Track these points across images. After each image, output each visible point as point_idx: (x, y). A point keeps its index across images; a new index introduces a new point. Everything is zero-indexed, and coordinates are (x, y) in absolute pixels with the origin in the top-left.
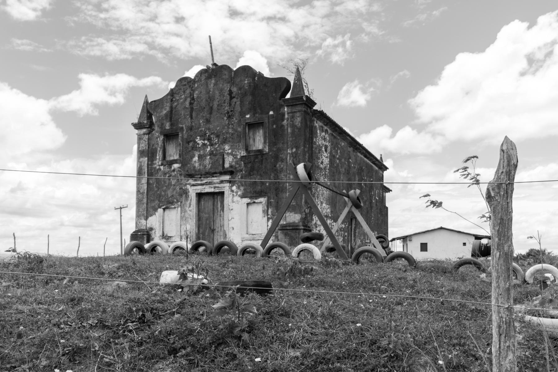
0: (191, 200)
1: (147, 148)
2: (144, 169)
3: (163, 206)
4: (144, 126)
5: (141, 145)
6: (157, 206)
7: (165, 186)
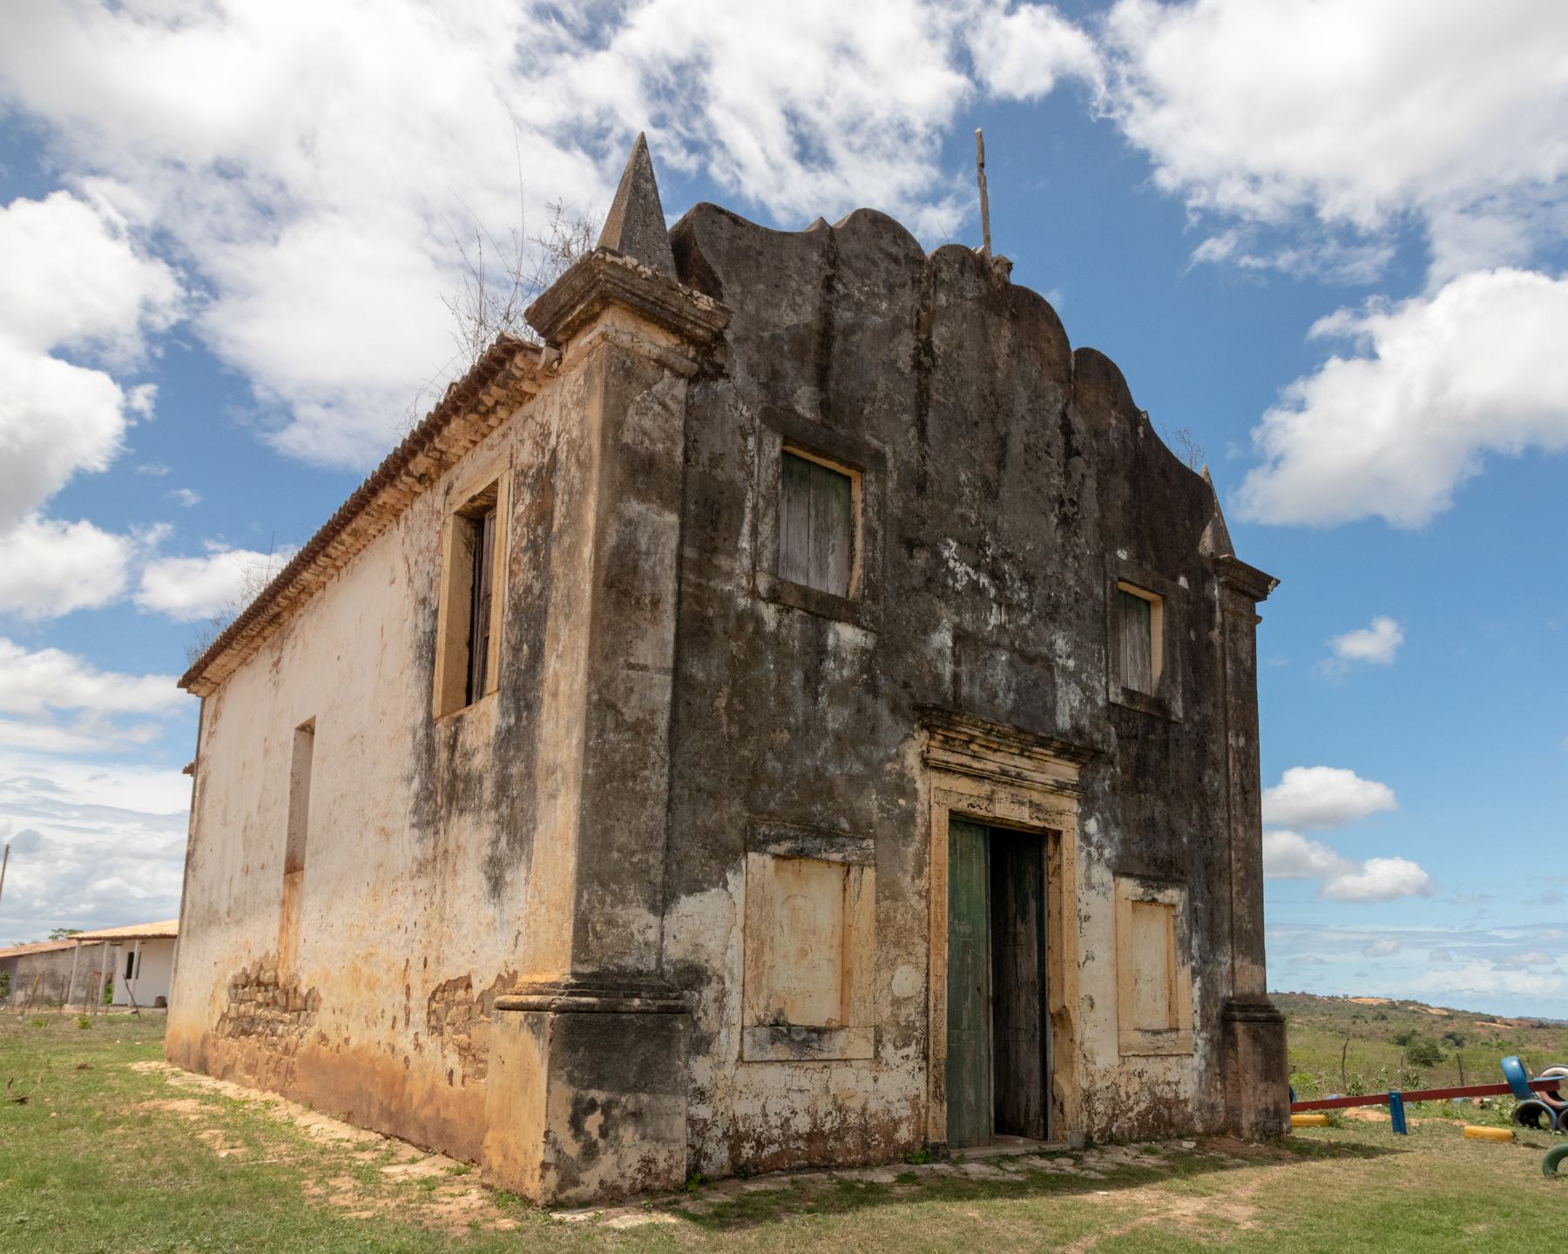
0: (928, 834)
3: (778, 840)
6: (734, 837)
7: (789, 730)
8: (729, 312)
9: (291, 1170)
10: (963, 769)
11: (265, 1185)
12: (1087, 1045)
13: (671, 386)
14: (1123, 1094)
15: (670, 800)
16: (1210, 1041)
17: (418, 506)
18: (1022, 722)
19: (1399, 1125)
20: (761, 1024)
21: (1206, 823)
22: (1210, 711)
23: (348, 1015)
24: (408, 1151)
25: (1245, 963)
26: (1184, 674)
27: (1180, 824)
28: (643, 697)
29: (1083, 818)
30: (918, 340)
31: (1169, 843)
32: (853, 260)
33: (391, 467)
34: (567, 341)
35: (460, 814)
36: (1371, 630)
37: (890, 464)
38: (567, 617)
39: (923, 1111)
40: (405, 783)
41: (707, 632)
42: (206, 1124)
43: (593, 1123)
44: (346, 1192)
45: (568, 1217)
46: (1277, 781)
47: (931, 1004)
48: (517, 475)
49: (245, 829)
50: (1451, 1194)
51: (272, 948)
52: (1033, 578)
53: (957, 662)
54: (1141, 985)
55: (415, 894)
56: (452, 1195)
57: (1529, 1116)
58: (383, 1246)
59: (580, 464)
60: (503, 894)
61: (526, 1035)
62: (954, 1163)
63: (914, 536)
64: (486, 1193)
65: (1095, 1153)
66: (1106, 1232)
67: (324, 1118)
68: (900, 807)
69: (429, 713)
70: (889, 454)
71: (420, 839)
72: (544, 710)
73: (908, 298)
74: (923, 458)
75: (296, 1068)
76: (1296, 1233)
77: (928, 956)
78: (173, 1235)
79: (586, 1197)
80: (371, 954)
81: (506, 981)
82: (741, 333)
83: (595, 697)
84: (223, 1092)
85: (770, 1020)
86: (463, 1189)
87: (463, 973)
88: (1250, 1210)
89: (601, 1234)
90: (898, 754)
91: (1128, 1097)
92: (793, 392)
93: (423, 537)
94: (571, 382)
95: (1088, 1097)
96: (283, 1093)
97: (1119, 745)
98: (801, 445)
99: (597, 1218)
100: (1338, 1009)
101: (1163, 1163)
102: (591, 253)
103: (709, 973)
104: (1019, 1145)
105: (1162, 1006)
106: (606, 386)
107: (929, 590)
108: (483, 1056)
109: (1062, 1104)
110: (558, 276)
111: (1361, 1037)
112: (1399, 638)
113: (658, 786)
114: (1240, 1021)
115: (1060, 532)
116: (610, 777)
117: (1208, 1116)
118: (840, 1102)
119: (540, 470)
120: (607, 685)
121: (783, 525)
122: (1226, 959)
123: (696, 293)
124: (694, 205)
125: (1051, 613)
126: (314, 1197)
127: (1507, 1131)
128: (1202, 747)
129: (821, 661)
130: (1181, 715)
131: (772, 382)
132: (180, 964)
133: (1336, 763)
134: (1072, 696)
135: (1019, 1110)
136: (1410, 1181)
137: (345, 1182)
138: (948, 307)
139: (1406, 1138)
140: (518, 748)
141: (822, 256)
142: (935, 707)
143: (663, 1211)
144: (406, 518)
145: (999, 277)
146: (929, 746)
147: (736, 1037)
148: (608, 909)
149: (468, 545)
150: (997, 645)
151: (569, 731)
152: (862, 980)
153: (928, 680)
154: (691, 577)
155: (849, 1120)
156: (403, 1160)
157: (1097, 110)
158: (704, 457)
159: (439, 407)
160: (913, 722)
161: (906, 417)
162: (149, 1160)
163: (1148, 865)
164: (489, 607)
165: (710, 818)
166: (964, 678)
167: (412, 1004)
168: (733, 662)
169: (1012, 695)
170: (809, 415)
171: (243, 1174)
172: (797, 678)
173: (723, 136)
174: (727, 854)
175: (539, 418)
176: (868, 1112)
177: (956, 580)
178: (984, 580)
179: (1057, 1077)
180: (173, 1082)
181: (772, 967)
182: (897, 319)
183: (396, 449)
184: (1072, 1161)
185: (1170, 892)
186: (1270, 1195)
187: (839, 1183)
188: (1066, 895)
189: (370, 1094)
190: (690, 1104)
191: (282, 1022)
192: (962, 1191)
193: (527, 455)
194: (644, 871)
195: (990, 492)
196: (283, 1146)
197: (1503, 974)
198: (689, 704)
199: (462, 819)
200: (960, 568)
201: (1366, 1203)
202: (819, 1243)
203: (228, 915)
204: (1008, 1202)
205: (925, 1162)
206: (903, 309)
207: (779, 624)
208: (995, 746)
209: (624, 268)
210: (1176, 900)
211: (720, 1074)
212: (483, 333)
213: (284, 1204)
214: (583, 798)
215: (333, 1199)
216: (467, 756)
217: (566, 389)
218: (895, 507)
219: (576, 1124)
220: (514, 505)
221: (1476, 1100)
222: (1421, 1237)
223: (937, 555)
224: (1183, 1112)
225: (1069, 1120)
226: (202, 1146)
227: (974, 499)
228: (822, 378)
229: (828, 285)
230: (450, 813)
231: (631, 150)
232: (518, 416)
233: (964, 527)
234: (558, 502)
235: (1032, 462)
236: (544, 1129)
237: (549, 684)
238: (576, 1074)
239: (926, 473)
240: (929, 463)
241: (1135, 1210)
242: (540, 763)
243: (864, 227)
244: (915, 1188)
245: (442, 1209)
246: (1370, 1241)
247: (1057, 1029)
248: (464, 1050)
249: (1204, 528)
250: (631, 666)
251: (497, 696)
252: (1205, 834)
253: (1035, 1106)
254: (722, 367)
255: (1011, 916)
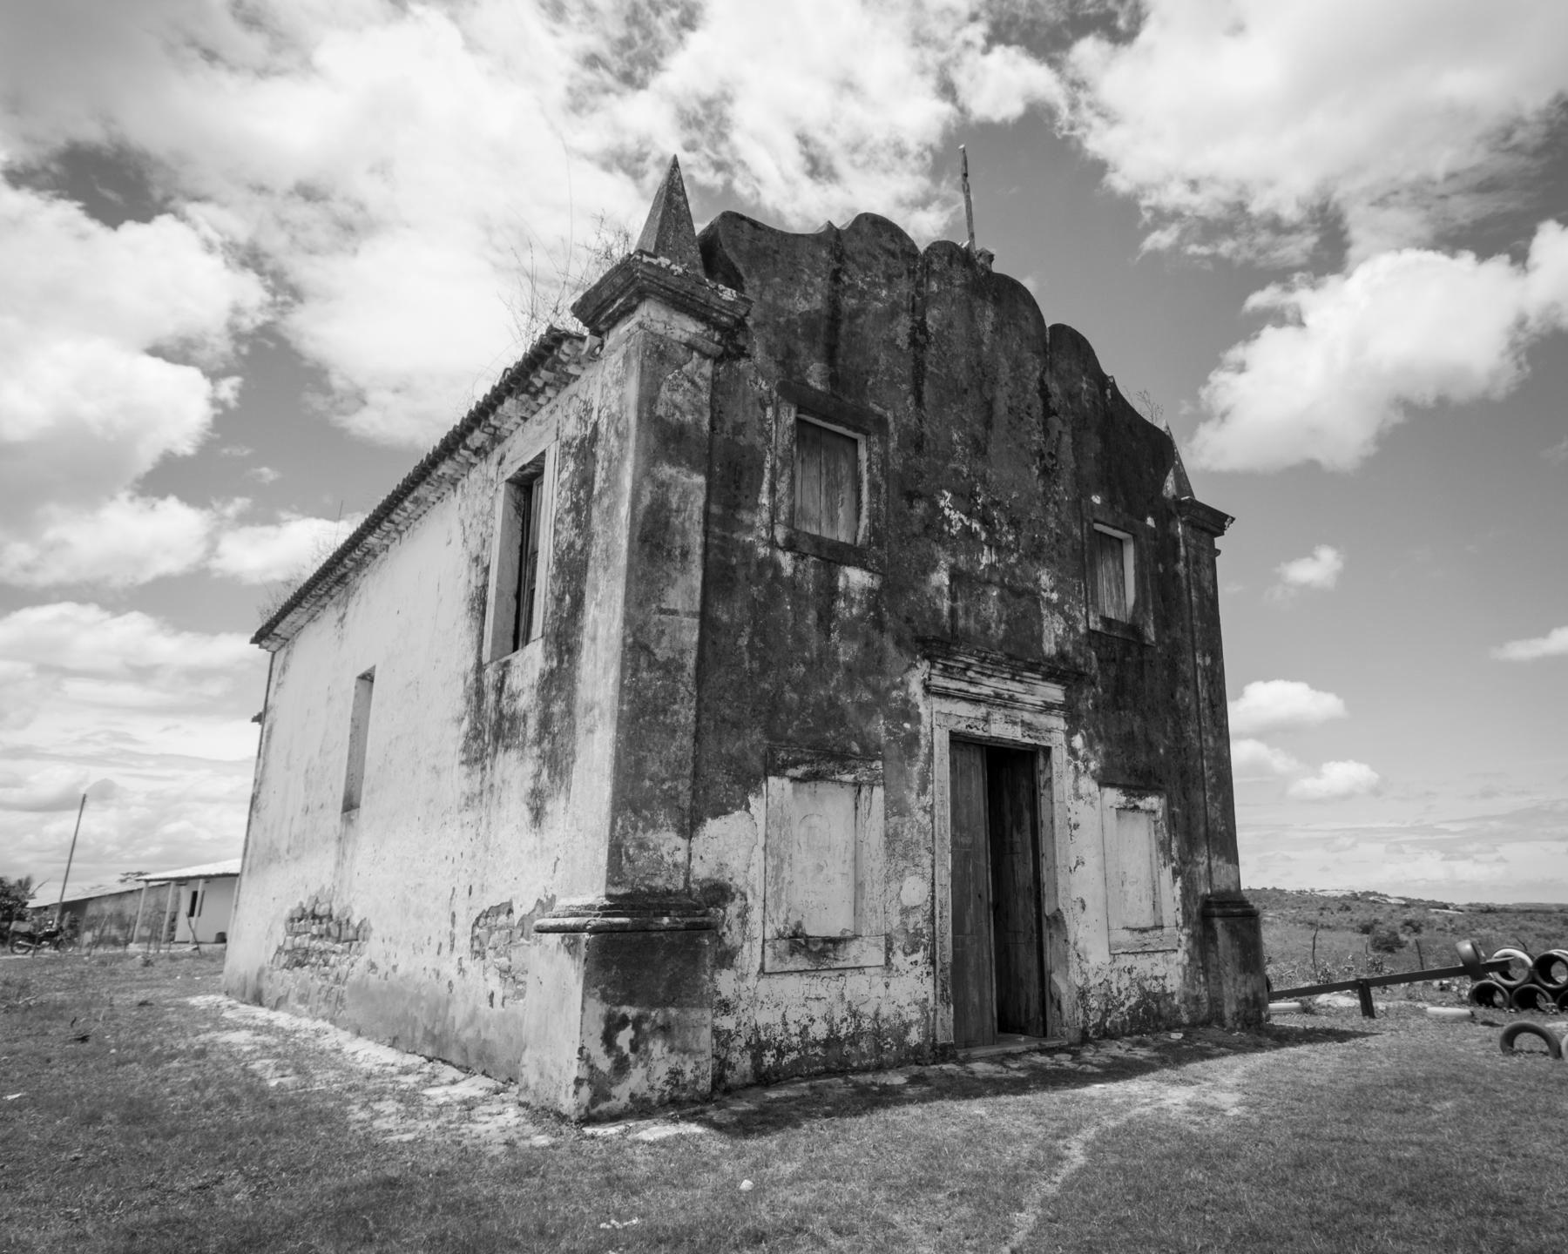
1: (706, 426)
2: (684, 534)
3: (795, 764)
4: (706, 306)
5: (665, 393)
8: (749, 302)
9: (338, 1096)
10: (961, 694)
11: (312, 1112)
12: (1080, 945)
13: (699, 366)
14: (1115, 990)
15: (698, 731)
16: (1191, 937)
17: (474, 475)
18: (1012, 650)
19: (1368, 1009)
20: (780, 936)
21: (1180, 736)
22: (1179, 635)
23: (397, 943)
24: (450, 1073)
25: (1220, 863)
26: (1154, 602)
27: (1156, 736)
28: (673, 638)
29: (1070, 734)
30: (914, 321)
31: (1148, 755)
32: (856, 255)
33: (450, 442)
34: (608, 330)
35: (506, 751)
36: (1315, 558)
37: (892, 427)
38: (606, 569)
39: (931, 1014)
40: (455, 724)
41: (731, 579)
42: (258, 1054)
43: (624, 1038)
44: (390, 1116)
45: (600, 1131)
46: (1240, 694)
47: (937, 912)
48: (562, 446)
49: (307, 771)
50: (1419, 1074)
51: (327, 882)
52: (1019, 522)
53: (954, 598)
54: (1127, 887)
55: (462, 826)
56: (490, 1114)
57: (1483, 996)
58: (423, 1168)
59: (618, 434)
60: (543, 824)
61: (563, 957)
62: (961, 1063)
63: (912, 489)
64: (522, 1111)
65: (1091, 1047)
66: (1104, 1124)
67: (371, 1043)
68: (905, 730)
69: (479, 659)
70: (891, 419)
71: (469, 775)
72: (584, 653)
73: (904, 287)
74: (920, 421)
75: (346, 996)
76: (1279, 1117)
77: (933, 867)
78: (222, 1166)
79: (617, 1111)
80: (420, 885)
81: (545, 905)
82: (760, 319)
83: (630, 640)
84: (276, 1023)
85: (789, 932)
86: (500, 1108)
87: (505, 900)
88: (1237, 1097)
89: (631, 1147)
90: (902, 683)
91: (1120, 992)
92: (807, 368)
93: (477, 502)
94: (612, 363)
95: (1083, 994)
96: (333, 1021)
97: (1100, 668)
98: (813, 414)
99: (628, 1131)
100: (1305, 902)
101: (1154, 1054)
102: (630, 255)
103: (733, 890)
104: (1020, 1044)
105: (1147, 905)
106: (642, 367)
107: (927, 535)
108: (521, 977)
109: (1059, 1002)
110: (601, 275)
111: (1329, 927)
112: (1339, 565)
113: (687, 718)
114: (1219, 916)
115: (1041, 482)
116: (643, 712)
117: (1193, 1008)
118: (854, 1008)
119: (583, 441)
120: (641, 629)
121: (798, 483)
122: (1203, 859)
123: (721, 287)
124: (719, 213)
125: (1036, 553)
126: (359, 1122)
127: (1466, 1011)
128: (1172, 666)
129: (833, 602)
130: (1153, 639)
131: (787, 360)
132: (241, 901)
133: (1290, 676)
134: (1056, 625)
135: (1019, 1009)
136: (1381, 1062)
137: (388, 1106)
138: (938, 293)
139: (1375, 1022)
140: (560, 689)
141: (830, 253)
142: (935, 639)
143: (690, 1121)
144: (463, 486)
145: (982, 266)
146: (930, 674)
147: (758, 950)
148: (640, 834)
149: (518, 508)
150: (989, 582)
151: (606, 671)
152: (873, 891)
153: (928, 614)
154: (717, 530)
155: (863, 1025)
156: (445, 1081)
157: (1061, 129)
158: (728, 426)
159: (494, 389)
160: (916, 653)
161: (904, 387)
162: (202, 1092)
163: (1130, 775)
164: (535, 562)
165: (733, 747)
166: (960, 613)
167: (457, 931)
168: (753, 605)
169: (1003, 626)
170: (819, 387)
171: (291, 1102)
172: (811, 617)
173: (743, 156)
174: (749, 778)
175: (582, 397)
176: (880, 1017)
177: (951, 526)
178: (976, 526)
179: (1053, 976)
180: (228, 1015)
181: (790, 883)
182: (895, 304)
183: (455, 427)
184: (1070, 1057)
185: (1149, 799)
186: (1254, 1081)
187: (854, 1087)
188: (1056, 805)
189: (415, 1019)
190: (715, 1016)
191: (334, 952)
192: (969, 1089)
193: (572, 429)
194: (672, 798)
195: (979, 449)
196: (331, 1073)
197: (1452, 863)
198: (714, 643)
199: (508, 754)
200: (955, 516)
201: (1341, 1085)
202: (836, 1146)
203: (288, 852)
204: (1012, 1098)
205: (934, 1063)
206: (900, 295)
207: (795, 569)
208: (989, 672)
209: (658, 267)
210: (1155, 806)
211: (743, 986)
212: (535, 325)
213: (330, 1131)
214: (618, 732)
215: (376, 1123)
216: (513, 697)
217: (607, 371)
218: (896, 463)
219: (608, 1039)
220: (560, 472)
221: (1436, 983)
222: (1395, 1116)
223: (933, 503)
224: (1170, 1006)
225: (1066, 1017)
226: (253, 1076)
227: (965, 456)
228: (830, 356)
229: (836, 277)
230: (496, 751)
231: (666, 169)
232: (564, 395)
233: (957, 479)
234: (599, 467)
235: (1015, 421)
236: (578, 1046)
237: (588, 629)
238: (609, 991)
239: (923, 434)
240: (925, 425)
241: (1130, 1102)
242: (579, 701)
243: (866, 228)
244: (925, 1089)
245: (479, 1128)
246: (1348, 1122)
247: (1052, 931)
248: (505, 972)
249: (1167, 474)
250: (662, 611)
251: (541, 642)
252: (1180, 748)
253: (1034, 1005)
254: (744, 348)
255: (1008, 824)
